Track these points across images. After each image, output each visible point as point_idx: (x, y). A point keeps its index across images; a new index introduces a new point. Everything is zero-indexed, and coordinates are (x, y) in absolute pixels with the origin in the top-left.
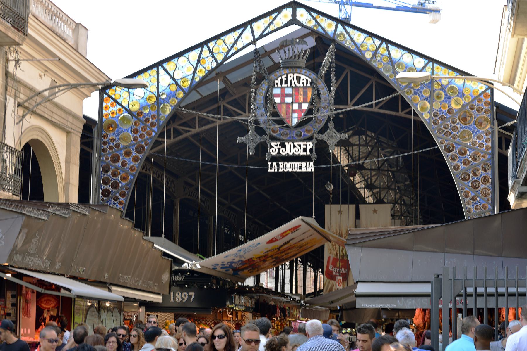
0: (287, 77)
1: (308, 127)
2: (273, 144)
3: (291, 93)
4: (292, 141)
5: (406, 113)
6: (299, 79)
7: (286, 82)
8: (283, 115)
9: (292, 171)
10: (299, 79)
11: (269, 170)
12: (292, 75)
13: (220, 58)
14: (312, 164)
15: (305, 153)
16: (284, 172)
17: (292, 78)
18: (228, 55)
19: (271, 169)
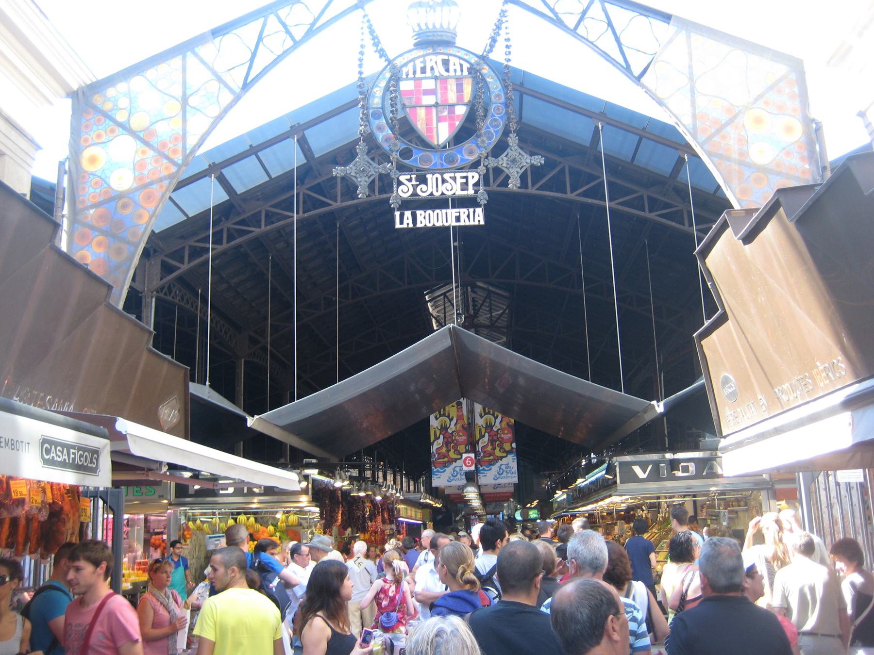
0: (424, 62)
1: (468, 145)
2: (403, 178)
4: (440, 171)
5: (579, 195)
6: (446, 63)
7: (423, 70)
8: (420, 126)
9: (441, 225)
10: (446, 63)
11: (398, 226)
12: (433, 57)
13: (298, 34)
14: (479, 211)
15: (464, 193)
16: (425, 227)
18: (314, 29)
19: (401, 222)
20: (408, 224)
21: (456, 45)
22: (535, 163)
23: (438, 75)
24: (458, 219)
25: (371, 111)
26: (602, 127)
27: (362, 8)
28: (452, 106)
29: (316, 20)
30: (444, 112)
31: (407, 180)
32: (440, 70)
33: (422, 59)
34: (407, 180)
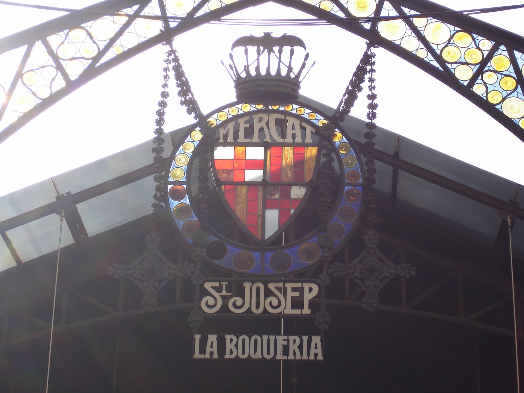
2: (208, 286)
3: (262, 158)
6: (281, 124)
7: (249, 133)
9: (261, 357)
11: (197, 355)
12: (265, 117)
14: (316, 340)
15: (298, 312)
17: (263, 124)
19: (202, 350)
20: (212, 353)
21: (298, 100)
22: (403, 274)
23: (269, 141)
24: (286, 350)
25: (170, 187)
26: (513, 222)
27: (169, 42)
28: (286, 188)
29: (101, 54)
30: (275, 194)
31: (213, 288)
32: (273, 132)
33: (247, 118)
34: (213, 288)
